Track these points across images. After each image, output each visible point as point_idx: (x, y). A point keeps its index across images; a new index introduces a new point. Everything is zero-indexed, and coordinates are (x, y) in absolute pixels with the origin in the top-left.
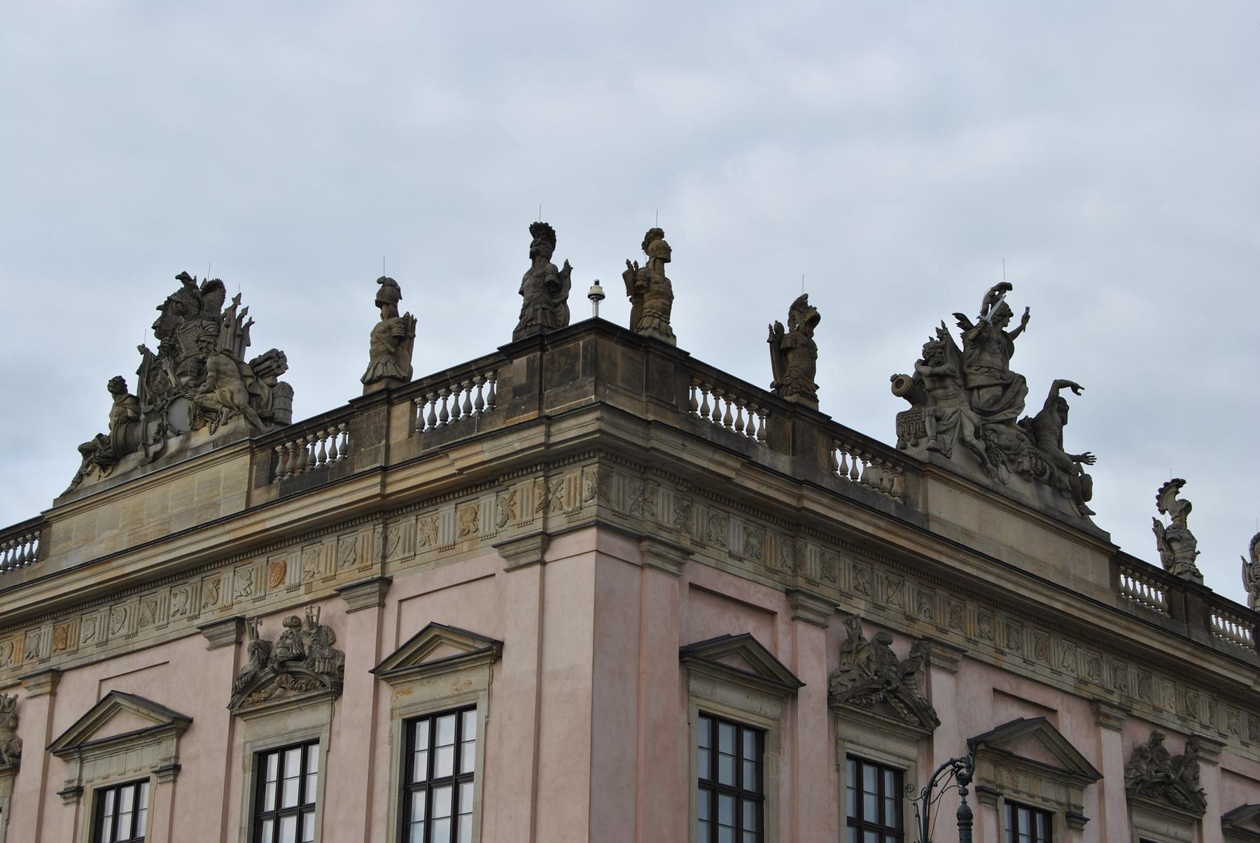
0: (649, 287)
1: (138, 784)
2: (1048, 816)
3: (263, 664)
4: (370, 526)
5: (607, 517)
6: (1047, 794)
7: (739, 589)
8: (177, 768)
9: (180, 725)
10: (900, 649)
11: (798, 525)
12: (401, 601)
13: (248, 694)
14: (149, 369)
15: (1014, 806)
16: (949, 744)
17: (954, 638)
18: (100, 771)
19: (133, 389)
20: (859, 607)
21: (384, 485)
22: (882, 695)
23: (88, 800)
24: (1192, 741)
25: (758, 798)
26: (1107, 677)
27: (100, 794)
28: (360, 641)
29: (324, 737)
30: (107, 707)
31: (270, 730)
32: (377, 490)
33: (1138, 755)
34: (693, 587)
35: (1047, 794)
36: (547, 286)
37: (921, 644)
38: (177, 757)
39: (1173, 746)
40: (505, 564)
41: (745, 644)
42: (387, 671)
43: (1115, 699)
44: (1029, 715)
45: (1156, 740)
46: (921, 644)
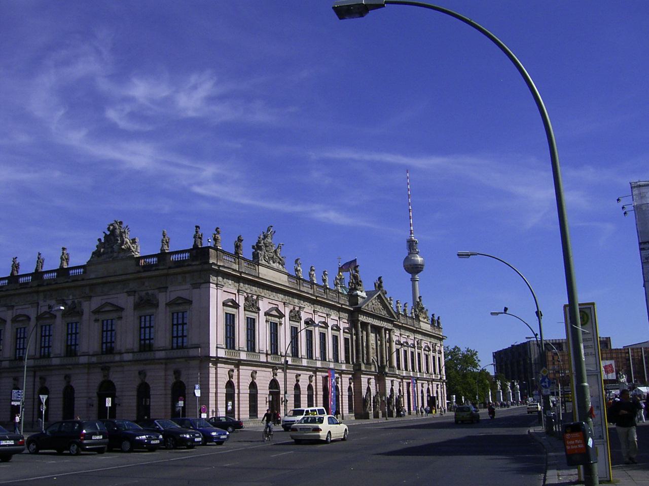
2: (277, 324)
3: (142, 300)
6: (276, 320)
9: (122, 309)
10: (255, 297)
13: (137, 306)
14: (106, 236)
15: (271, 322)
16: (262, 313)
17: (263, 295)
19: (103, 241)
20: (248, 291)
22: (252, 305)
23: (100, 322)
24: (300, 307)
26: (287, 299)
28: (163, 299)
29: (155, 314)
33: (291, 312)
34: (224, 291)
35: (276, 320)
36: (198, 237)
37: (258, 296)
39: (297, 309)
42: (168, 305)
43: (288, 302)
44: (274, 306)
45: (294, 309)
46: (258, 296)
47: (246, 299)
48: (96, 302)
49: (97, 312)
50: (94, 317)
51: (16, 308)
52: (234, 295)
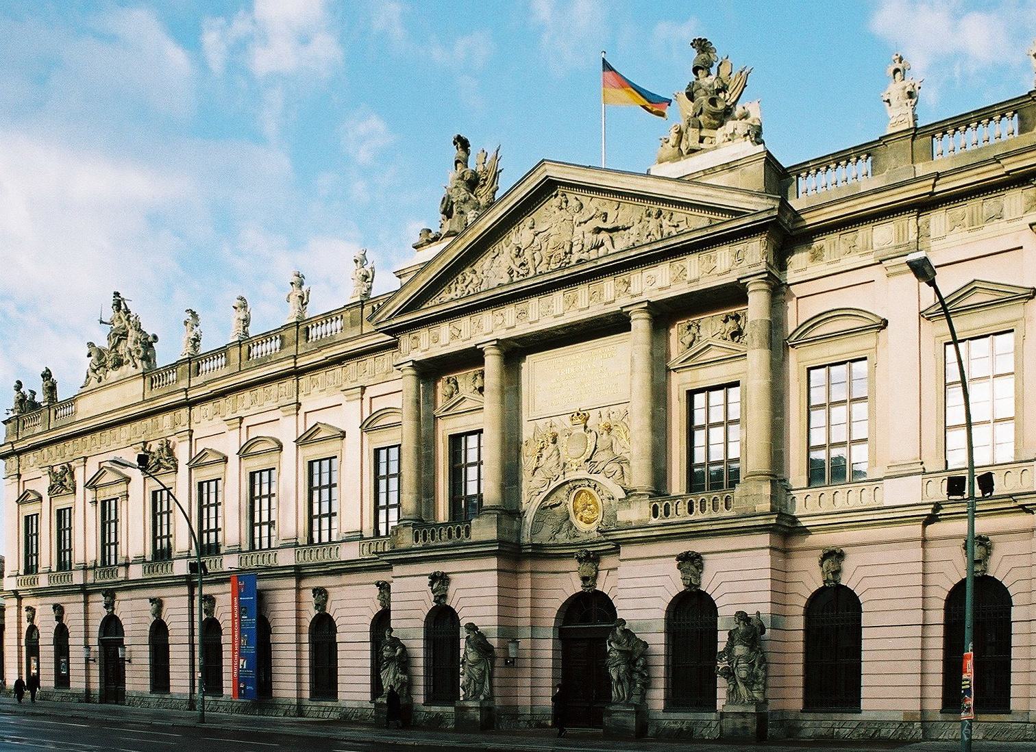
1: (116, 499)
4: (184, 410)
8: (127, 496)
18: (104, 494)
27: (104, 503)
28: (182, 453)
38: (127, 491)
49: (92, 485)
50: (90, 494)
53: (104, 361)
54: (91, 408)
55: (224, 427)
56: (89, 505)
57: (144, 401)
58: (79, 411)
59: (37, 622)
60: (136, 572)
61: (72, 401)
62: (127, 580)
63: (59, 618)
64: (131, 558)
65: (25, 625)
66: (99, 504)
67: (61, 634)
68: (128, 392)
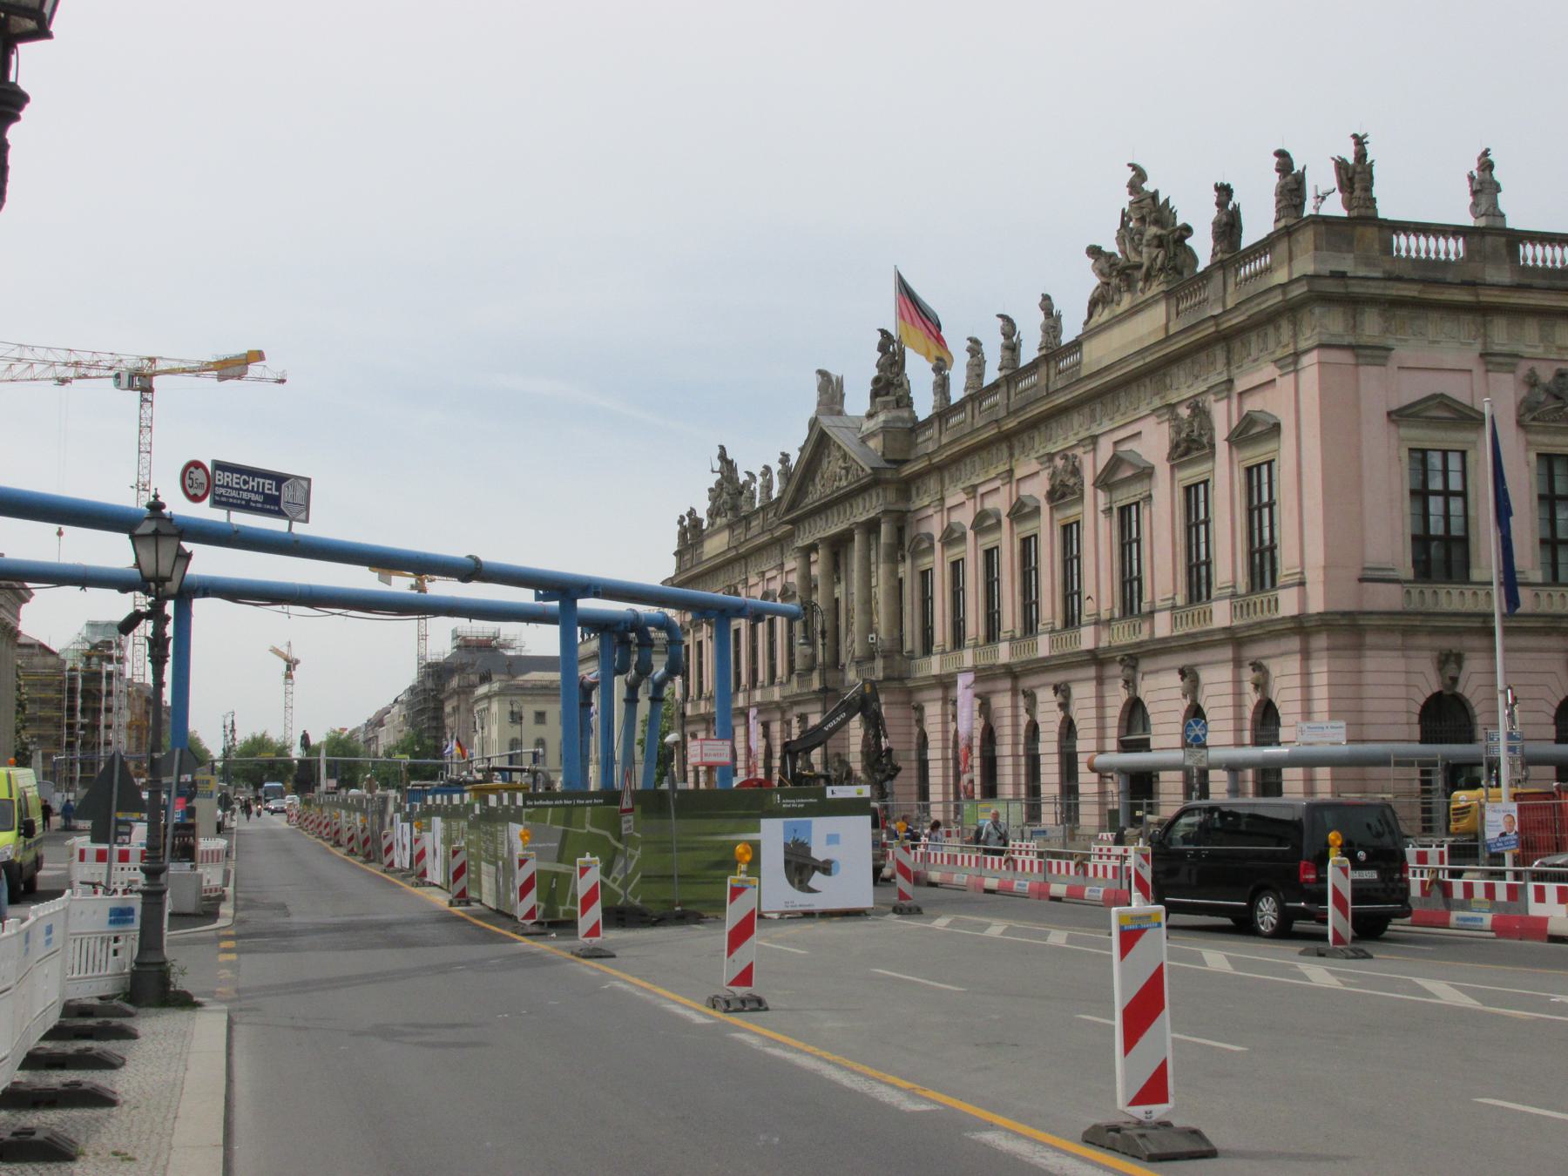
0: (1355, 176)
1: (1137, 504)
5: (1325, 339)
7: (1438, 361)
8: (1150, 496)
9: (1146, 473)
11: (1484, 311)
12: (1241, 394)
18: (1124, 497)
21: (1217, 325)
25: (1463, 494)
30: (1116, 462)
31: (1190, 474)
32: (1212, 330)
40: (1278, 372)
41: (1441, 400)
47: (1532, 381)
48: (1105, 452)
49: (1106, 481)
51: (982, 490)
52: (1464, 378)
53: (1116, 275)
54: (1102, 352)
55: (1268, 371)
56: (1101, 516)
57: (1168, 338)
58: (1086, 359)
59: (1040, 718)
60: (1163, 626)
61: (1076, 345)
62: (1153, 640)
63: (1064, 706)
64: (1158, 604)
65: (1024, 719)
66: (1115, 511)
67: (1068, 730)
68: (1146, 326)
